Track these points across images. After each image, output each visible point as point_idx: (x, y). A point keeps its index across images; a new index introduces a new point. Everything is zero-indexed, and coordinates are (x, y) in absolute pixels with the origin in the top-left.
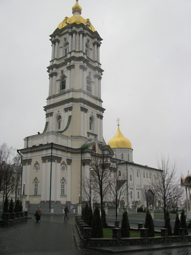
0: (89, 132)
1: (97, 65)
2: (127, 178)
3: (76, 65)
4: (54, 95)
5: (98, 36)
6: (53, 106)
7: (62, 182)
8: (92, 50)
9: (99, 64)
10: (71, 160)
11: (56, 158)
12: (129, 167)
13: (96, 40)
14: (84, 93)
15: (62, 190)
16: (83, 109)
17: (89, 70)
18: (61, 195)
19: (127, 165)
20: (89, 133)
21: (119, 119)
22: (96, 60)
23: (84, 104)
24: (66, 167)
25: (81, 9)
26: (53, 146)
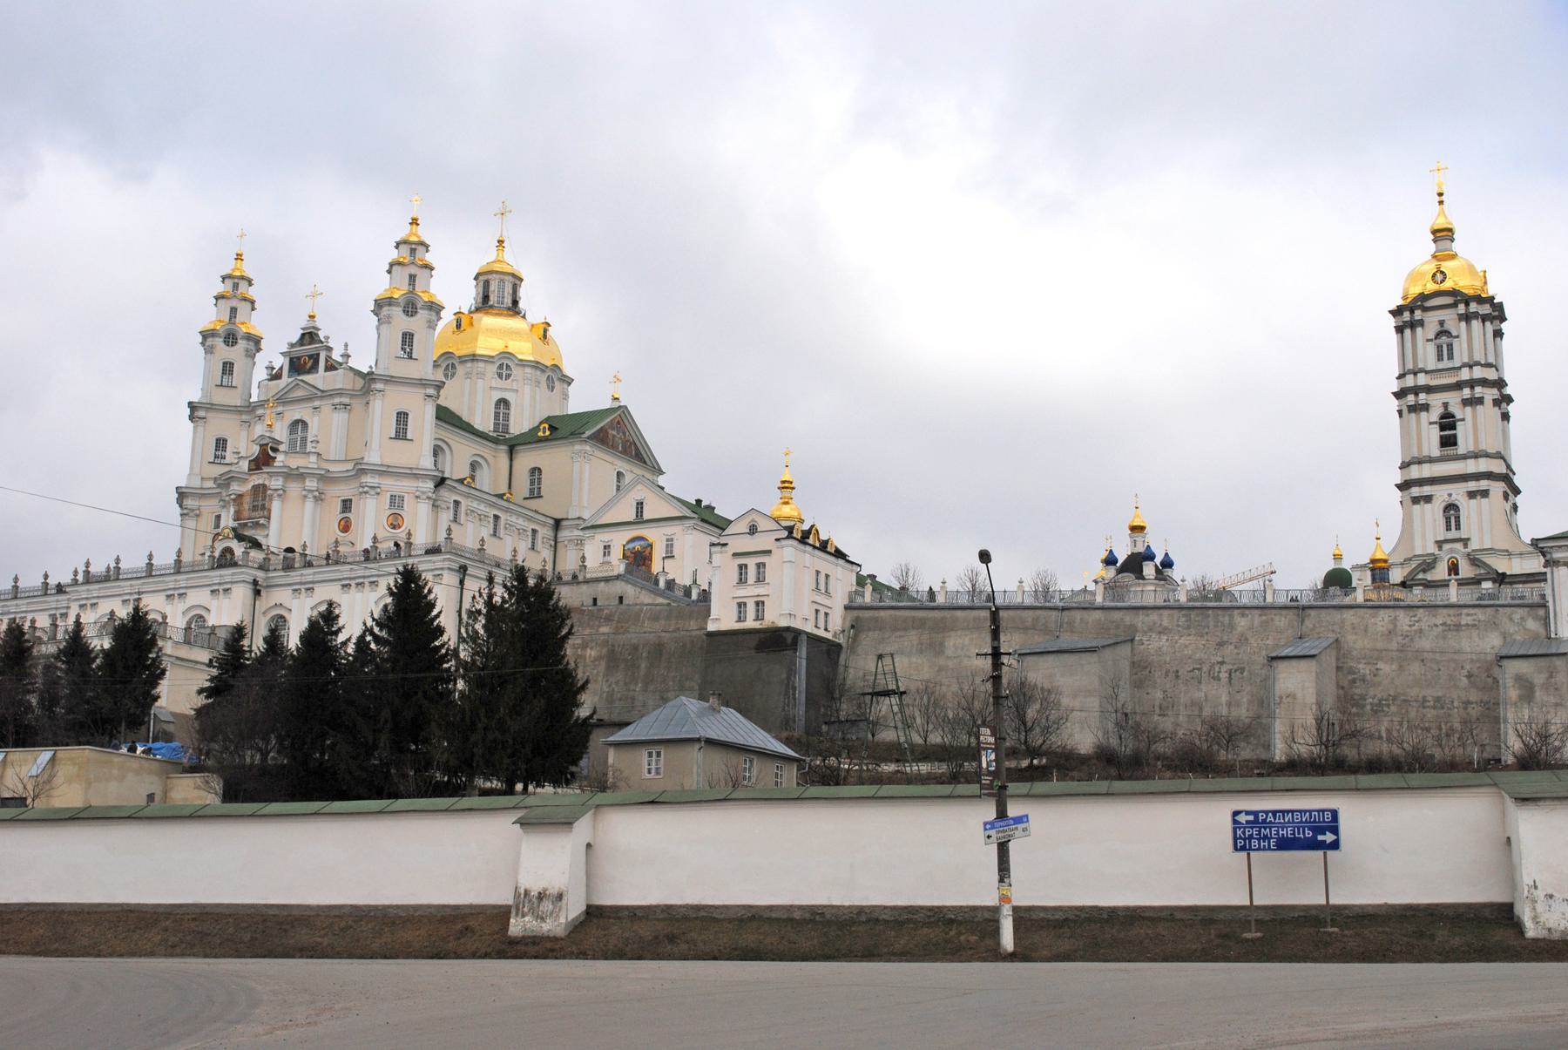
13: (1461, 308)
17: (1436, 400)
20: (1440, 544)
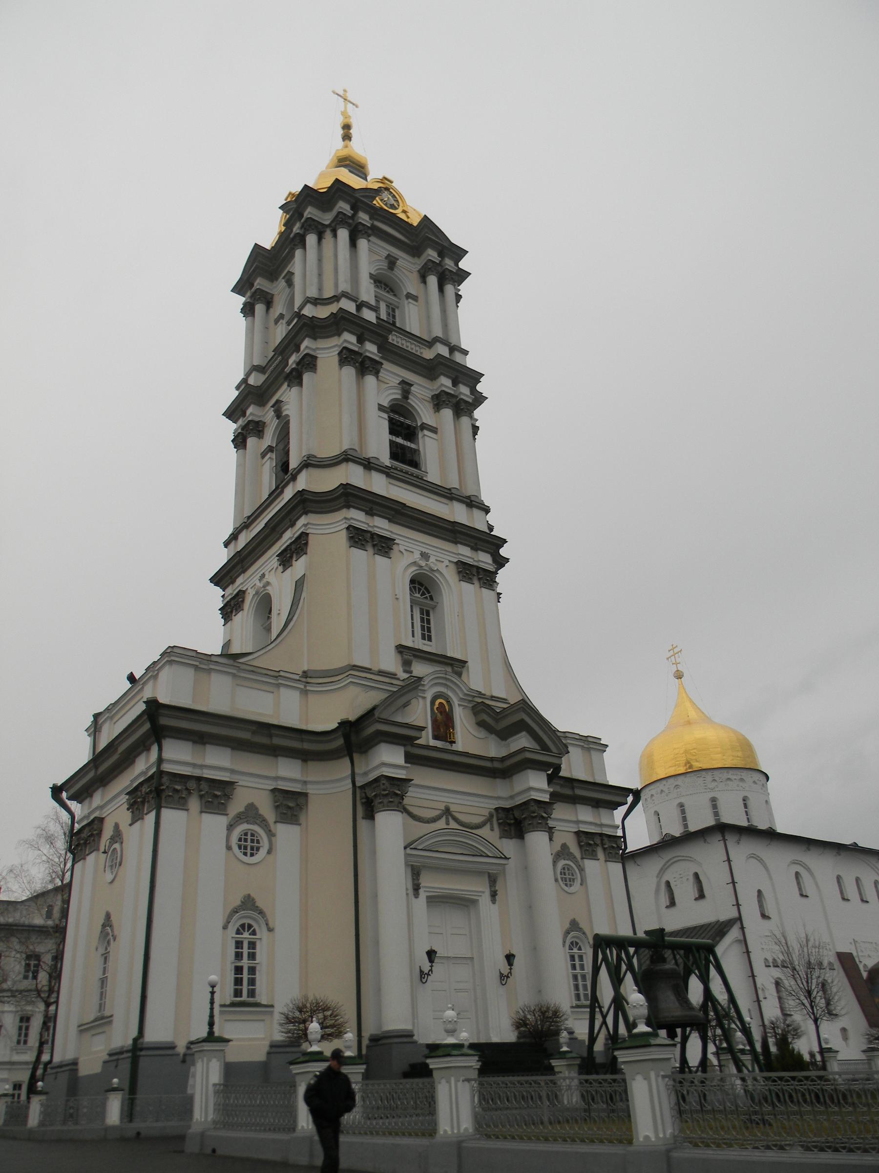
0: (404, 643)
1: (444, 351)
2: (738, 905)
3: (320, 355)
4: (249, 517)
5: (437, 237)
6: (242, 561)
7: (243, 926)
8: (415, 298)
9: (454, 349)
10: (306, 795)
11: (192, 785)
12: (741, 851)
13: (432, 254)
14: (369, 465)
15: (238, 970)
16: (358, 537)
18: (233, 1005)
19: (725, 840)
21: (676, 650)
22: (440, 335)
23: (370, 513)
24: (271, 834)
25: (362, 161)
26: (164, 721)
